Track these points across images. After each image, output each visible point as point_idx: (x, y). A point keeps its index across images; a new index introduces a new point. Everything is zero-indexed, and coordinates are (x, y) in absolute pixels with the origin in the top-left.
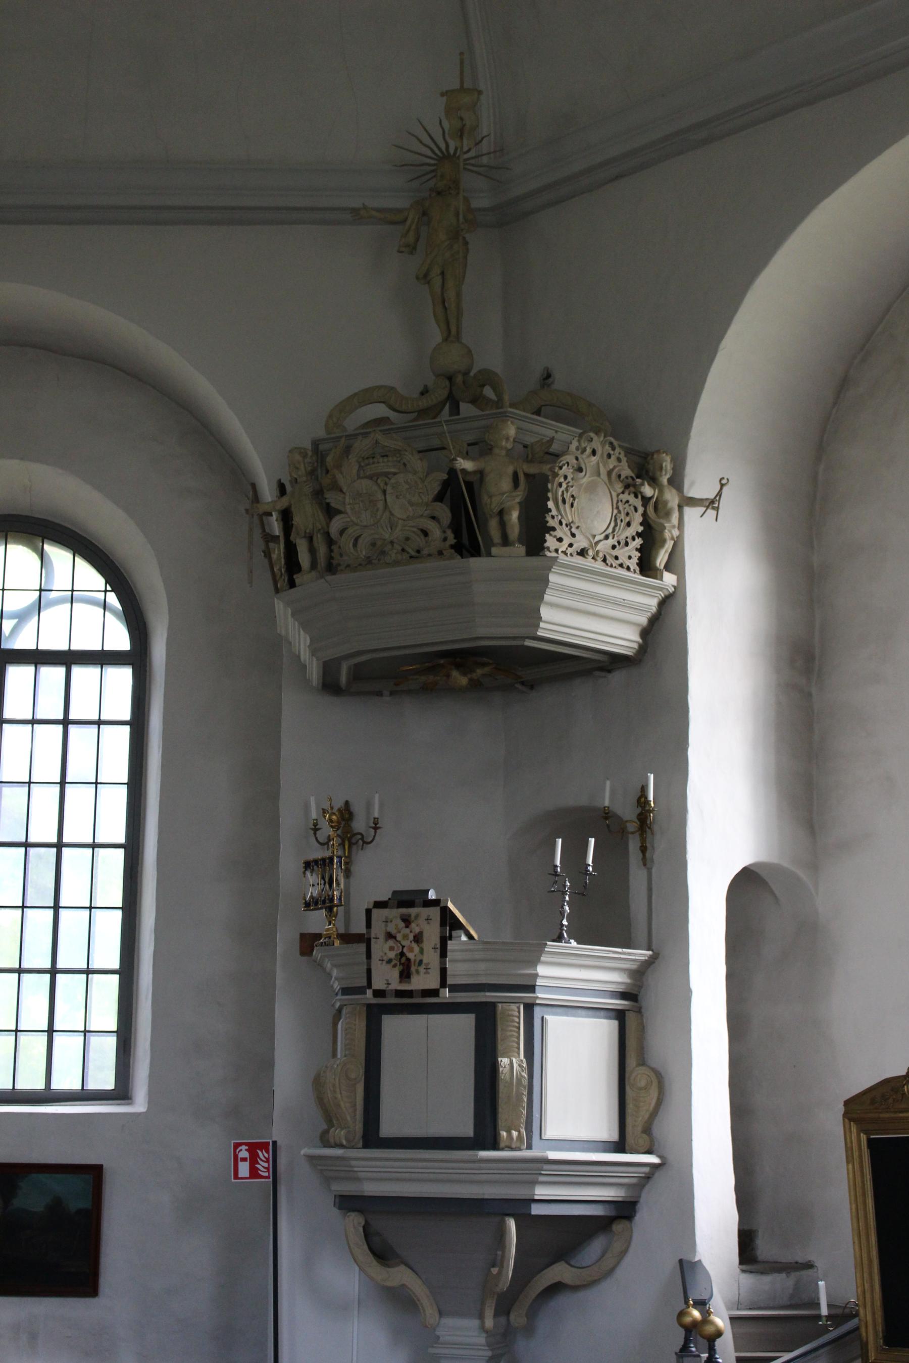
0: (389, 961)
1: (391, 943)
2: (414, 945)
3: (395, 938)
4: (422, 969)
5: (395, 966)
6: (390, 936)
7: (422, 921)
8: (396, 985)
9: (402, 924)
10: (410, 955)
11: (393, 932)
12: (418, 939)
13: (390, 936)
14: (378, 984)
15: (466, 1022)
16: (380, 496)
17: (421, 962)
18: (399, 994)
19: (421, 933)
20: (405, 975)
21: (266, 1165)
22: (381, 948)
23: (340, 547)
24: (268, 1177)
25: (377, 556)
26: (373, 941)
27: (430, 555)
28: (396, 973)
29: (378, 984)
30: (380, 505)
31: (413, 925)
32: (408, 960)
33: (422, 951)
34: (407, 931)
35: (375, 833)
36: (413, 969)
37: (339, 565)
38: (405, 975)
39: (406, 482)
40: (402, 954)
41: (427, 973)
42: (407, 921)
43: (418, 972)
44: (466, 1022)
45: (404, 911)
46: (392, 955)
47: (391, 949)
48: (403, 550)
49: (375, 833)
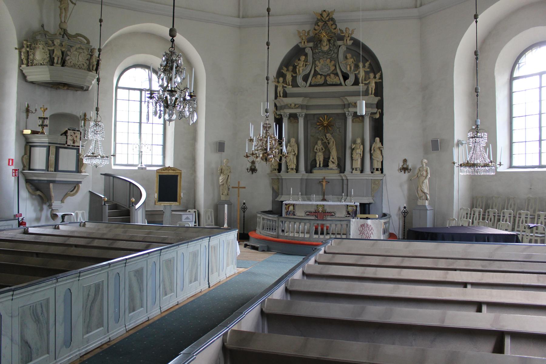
12: (76, 137)
14: (68, 144)
15: (75, 151)
20: (74, 143)
22: (69, 137)
25: (74, 66)
29: (68, 144)
38: (74, 143)
42: (74, 133)
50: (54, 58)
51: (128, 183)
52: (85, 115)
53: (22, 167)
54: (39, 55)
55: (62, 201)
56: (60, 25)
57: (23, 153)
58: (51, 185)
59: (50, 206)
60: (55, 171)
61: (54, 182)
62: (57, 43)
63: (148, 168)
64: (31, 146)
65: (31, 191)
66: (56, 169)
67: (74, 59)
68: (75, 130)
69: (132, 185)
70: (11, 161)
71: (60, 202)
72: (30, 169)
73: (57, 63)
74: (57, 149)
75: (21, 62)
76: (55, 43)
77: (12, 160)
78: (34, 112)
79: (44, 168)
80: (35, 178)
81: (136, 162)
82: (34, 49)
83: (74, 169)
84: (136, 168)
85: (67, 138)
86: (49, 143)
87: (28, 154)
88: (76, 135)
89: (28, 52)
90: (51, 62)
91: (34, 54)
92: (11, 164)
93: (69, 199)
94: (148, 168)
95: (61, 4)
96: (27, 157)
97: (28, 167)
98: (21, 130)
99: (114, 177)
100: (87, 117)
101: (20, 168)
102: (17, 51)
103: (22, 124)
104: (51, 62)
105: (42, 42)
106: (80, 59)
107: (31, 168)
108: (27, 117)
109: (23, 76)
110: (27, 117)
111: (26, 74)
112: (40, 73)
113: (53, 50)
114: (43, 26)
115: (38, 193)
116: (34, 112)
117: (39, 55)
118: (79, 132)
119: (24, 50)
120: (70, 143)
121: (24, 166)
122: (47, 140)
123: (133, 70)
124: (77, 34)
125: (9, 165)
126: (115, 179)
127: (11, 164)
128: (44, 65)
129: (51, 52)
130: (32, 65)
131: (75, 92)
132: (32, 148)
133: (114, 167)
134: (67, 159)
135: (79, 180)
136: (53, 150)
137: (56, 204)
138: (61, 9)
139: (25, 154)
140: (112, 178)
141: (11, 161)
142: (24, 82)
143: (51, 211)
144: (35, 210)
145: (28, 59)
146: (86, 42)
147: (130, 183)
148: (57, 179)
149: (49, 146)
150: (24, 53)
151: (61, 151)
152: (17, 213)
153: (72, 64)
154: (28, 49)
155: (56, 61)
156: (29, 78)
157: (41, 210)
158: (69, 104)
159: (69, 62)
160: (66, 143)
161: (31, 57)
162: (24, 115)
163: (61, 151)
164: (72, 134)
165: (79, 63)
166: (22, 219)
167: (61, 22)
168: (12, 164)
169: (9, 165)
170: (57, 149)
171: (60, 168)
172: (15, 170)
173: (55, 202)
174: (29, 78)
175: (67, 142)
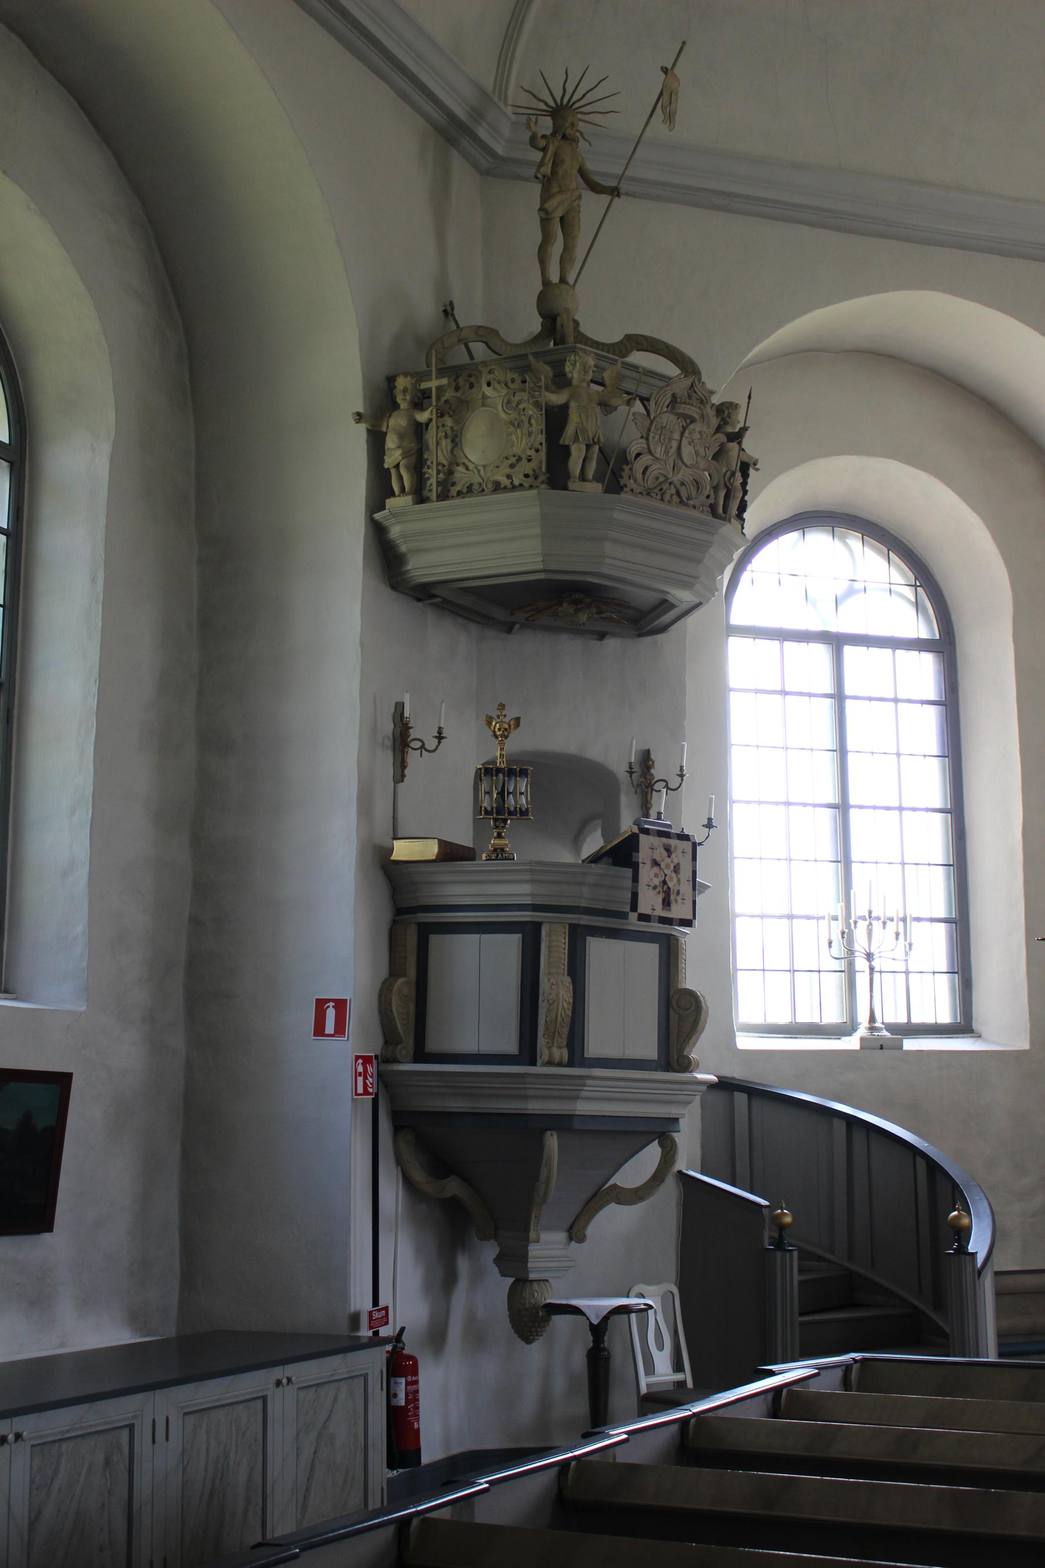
0: (655, 888)
1: (656, 869)
2: (674, 875)
3: (659, 865)
4: (679, 898)
5: (659, 893)
6: (655, 863)
7: (679, 852)
8: (660, 912)
9: (665, 854)
10: (670, 884)
11: (658, 859)
12: (676, 869)
13: (655, 863)
14: (643, 908)
15: (652, 950)
16: (676, 436)
17: (678, 893)
18: (664, 920)
19: (678, 864)
20: (667, 903)
21: (371, 1080)
22: (647, 873)
23: (631, 469)
24: (371, 1094)
25: (657, 490)
26: (641, 865)
27: (694, 507)
28: (660, 899)
29: (643, 908)
30: (675, 444)
31: (673, 856)
32: (669, 888)
33: (679, 881)
34: (668, 860)
35: (439, 743)
36: (672, 897)
37: (626, 486)
38: (667, 903)
39: (700, 432)
40: (664, 882)
41: (683, 903)
42: (668, 850)
43: (676, 901)
44: (652, 950)
45: (665, 840)
46: (657, 881)
47: (656, 875)
48: (678, 493)
49: (439, 743)
50: (566, 451)
51: (840, 1126)
52: (646, 760)
53: (380, 1041)
54: (489, 437)
55: (575, 1233)
56: (542, 299)
57: (384, 972)
58: (552, 1141)
59: (513, 1260)
60: (571, 1064)
61: (563, 1123)
62: (585, 369)
63: (910, 1044)
64: (426, 931)
65: (419, 1176)
66: (576, 1054)
67: (659, 451)
68: (667, 835)
69: (859, 1137)
70: (331, 1014)
71: (562, 1236)
72: (421, 1055)
73: (583, 477)
74: (577, 937)
75: (381, 487)
76: (574, 371)
77: (341, 1005)
78: (431, 743)
79: (511, 1047)
80: (457, 1105)
81: (833, 1015)
82: (456, 410)
83: (650, 1051)
84: (851, 1043)
85: (635, 879)
86: (535, 908)
87: (412, 972)
88: (676, 857)
89: (419, 430)
90: (556, 473)
91: (456, 440)
92: (330, 1027)
93: (613, 1222)
94: (910, 1044)
95: (546, 195)
96: (403, 986)
97: (409, 1041)
98: (382, 835)
99: (754, 1093)
100: (657, 772)
101: (374, 1047)
102: (360, 433)
103: (382, 809)
104: (556, 473)
105: (499, 374)
106: (687, 451)
107: (433, 1045)
108: (400, 776)
109: (387, 558)
110: (400, 776)
111: (403, 548)
112: (490, 537)
113: (564, 408)
114: (448, 312)
115: (453, 1187)
116: (431, 743)
117: (489, 437)
118: (687, 846)
119: (397, 422)
120: (650, 902)
121: (390, 1037)
122: (526, 888)
123: (789, 540)
124: (628, 337)
125: (319, 1030)
126: (757, 1104)
127: (330, 1027)
128: (514, 488)
129: (556, 420)
130: (443, 496)
131: (595, 644)
132: (434, 939)
133: (745, 1042)
134: (619, 992)
135: (672, 1111)
136: (554, 945)
137: (546, 1248)
138: (545, 221)
139: (395, 970)
140: (741, 1098)
141: (331, 1014)
142: (387, 591)
143: (513, 1294)
144: (428, 1287)
145: (418, 467)
146: (671, 370)
147: (851, 1121)
148: (582, 1108)
149: (537, 926)
150: (401, 436)
151: (598, 949)
152: (368, 1305)
153: (650, 483)
154: (423, 417)
155: (575, 465)
156: (422, 567)
157: (449, 1281)
158: (575, 708)
159: (638, 466)
160: (634, 907)
161: (438, 453)
162: (386, 761)
163: (598, 949)
164: (660, 854)
165: (677, 478)
166: (398, 1338)
167: (546, 283)
168: (340, 1028)
169: (319, 1030)
170: (577, 937)
171: (595, 1046)
172: (367, 1060)
173: (544, 1236)
174: (422, 567)
175: (635, 896)
